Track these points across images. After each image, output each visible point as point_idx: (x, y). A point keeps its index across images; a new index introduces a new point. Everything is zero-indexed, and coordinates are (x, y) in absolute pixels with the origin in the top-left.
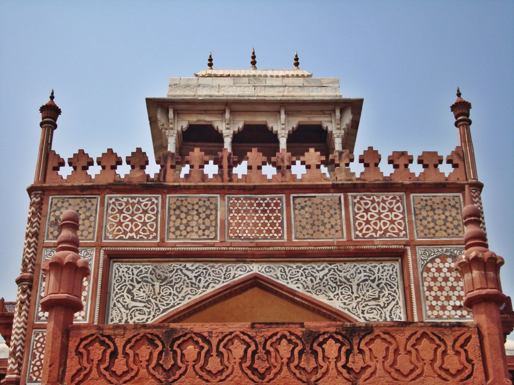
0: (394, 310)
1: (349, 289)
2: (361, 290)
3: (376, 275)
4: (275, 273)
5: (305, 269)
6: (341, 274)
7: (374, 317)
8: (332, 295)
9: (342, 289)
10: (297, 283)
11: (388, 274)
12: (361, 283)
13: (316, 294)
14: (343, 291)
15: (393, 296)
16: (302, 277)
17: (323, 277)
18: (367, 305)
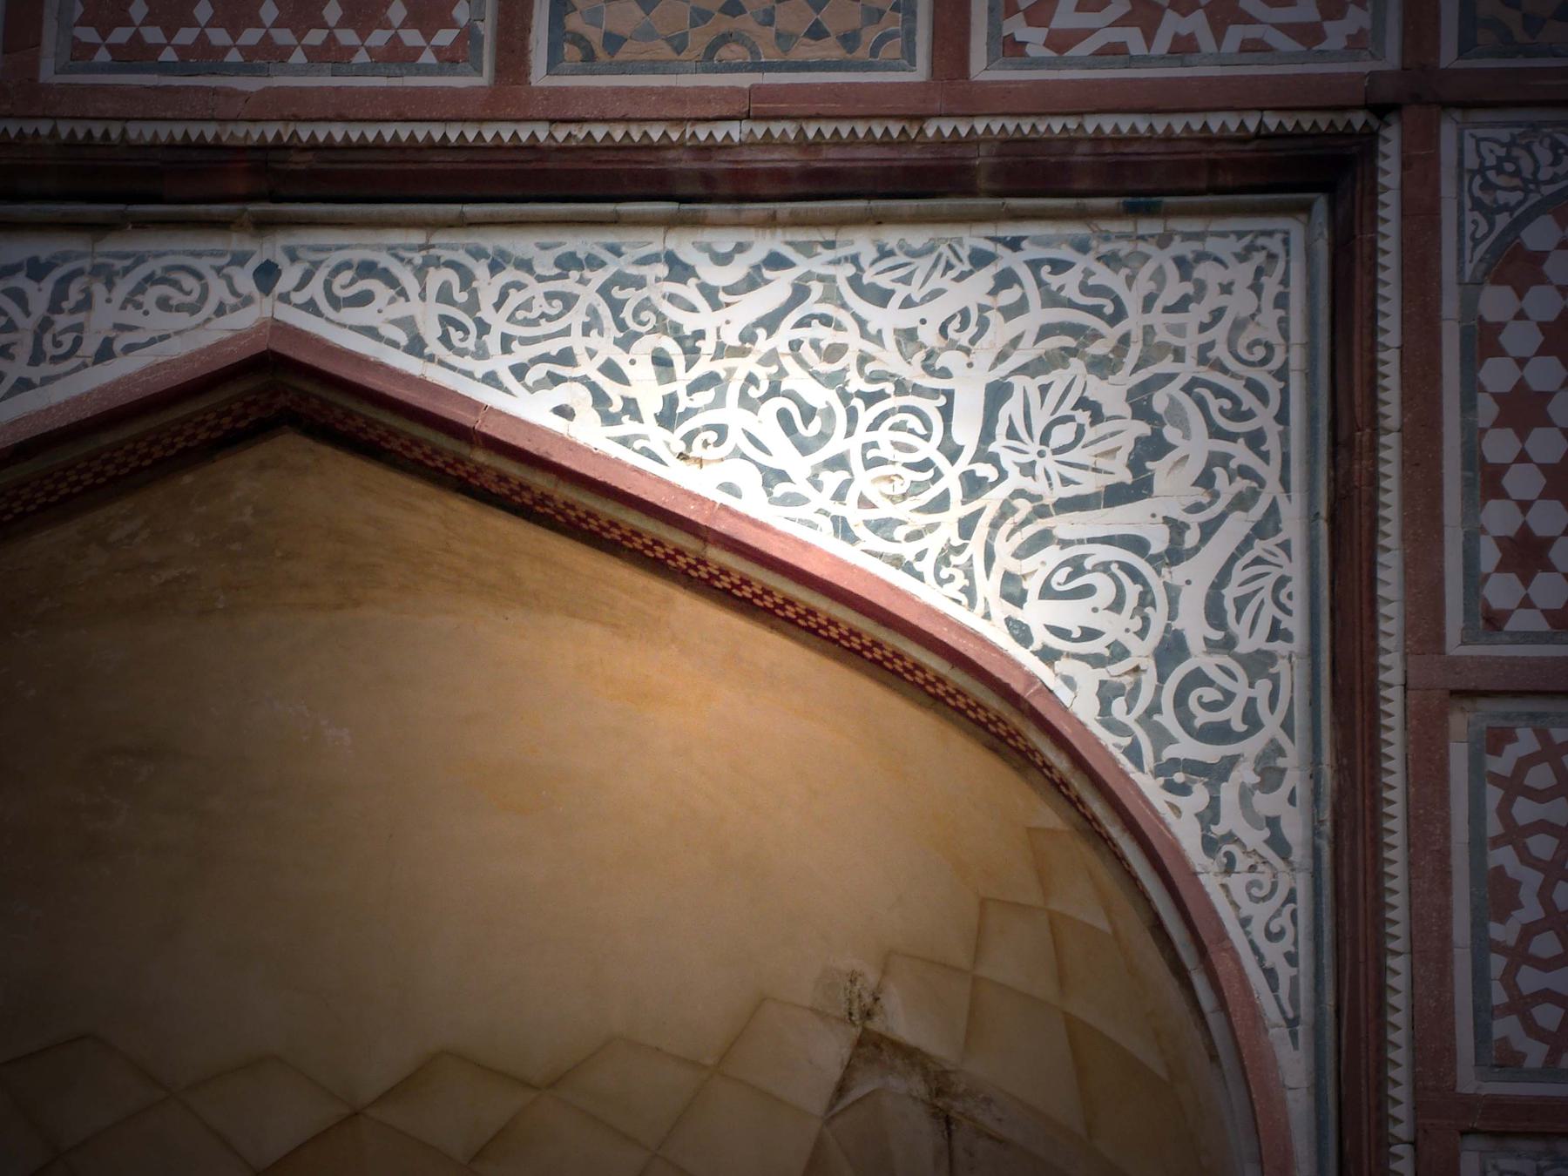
0: (1238, 574)
1: (927, 424)
2: (1012, 433)
3: (1133, 323)
4: (401, 309)
5: (621, 280)
6: (877, 317)
7: (1094, 622)
8: (798, 466)
9: (874, 426)
10: (555, 380)
11: (1217, 314)
12: (1019, 382)
13: (682, 456)
14: (884, 435)
15: (1244, 472)
16: (594, 340)
17: (748, 336)
18: (1043, 539)
